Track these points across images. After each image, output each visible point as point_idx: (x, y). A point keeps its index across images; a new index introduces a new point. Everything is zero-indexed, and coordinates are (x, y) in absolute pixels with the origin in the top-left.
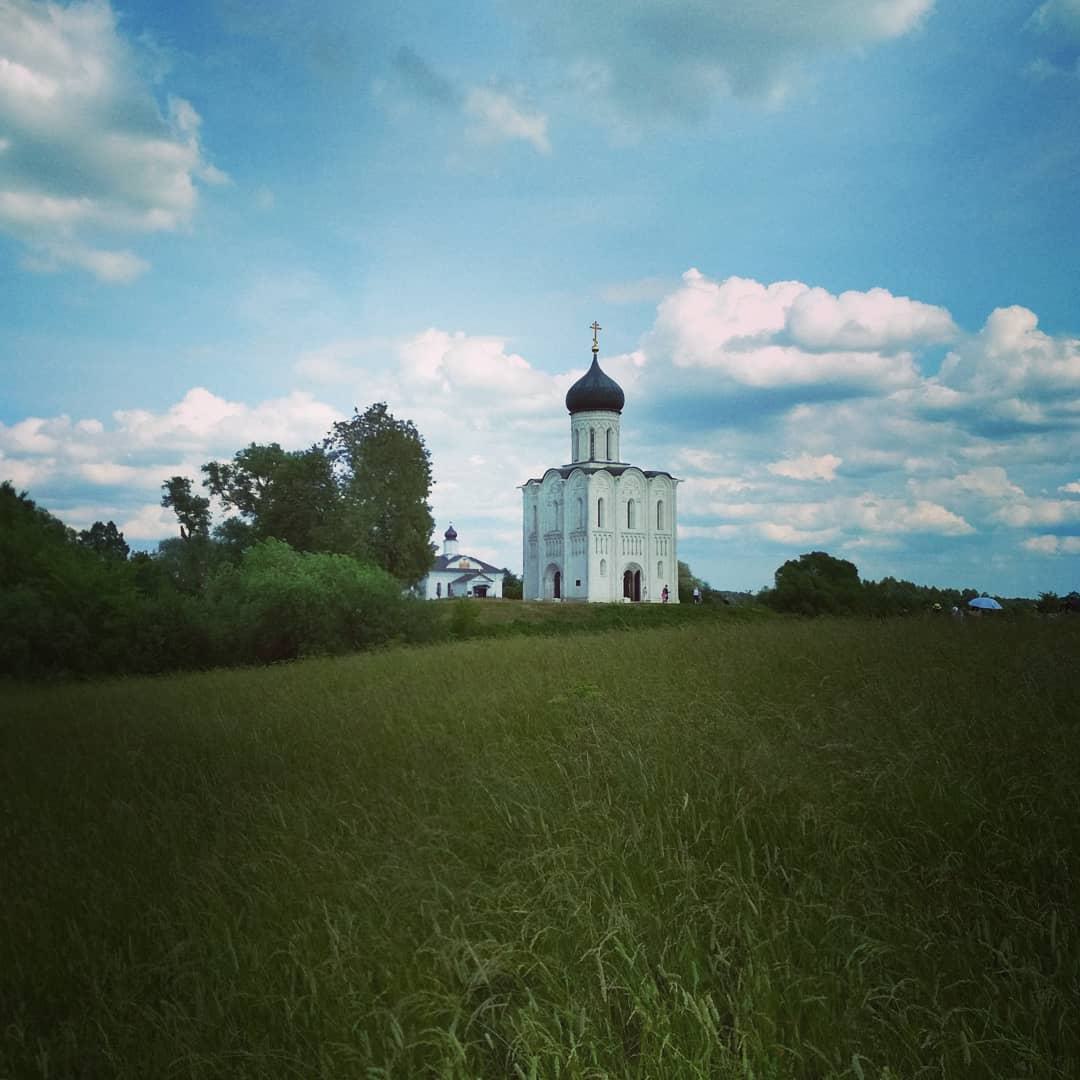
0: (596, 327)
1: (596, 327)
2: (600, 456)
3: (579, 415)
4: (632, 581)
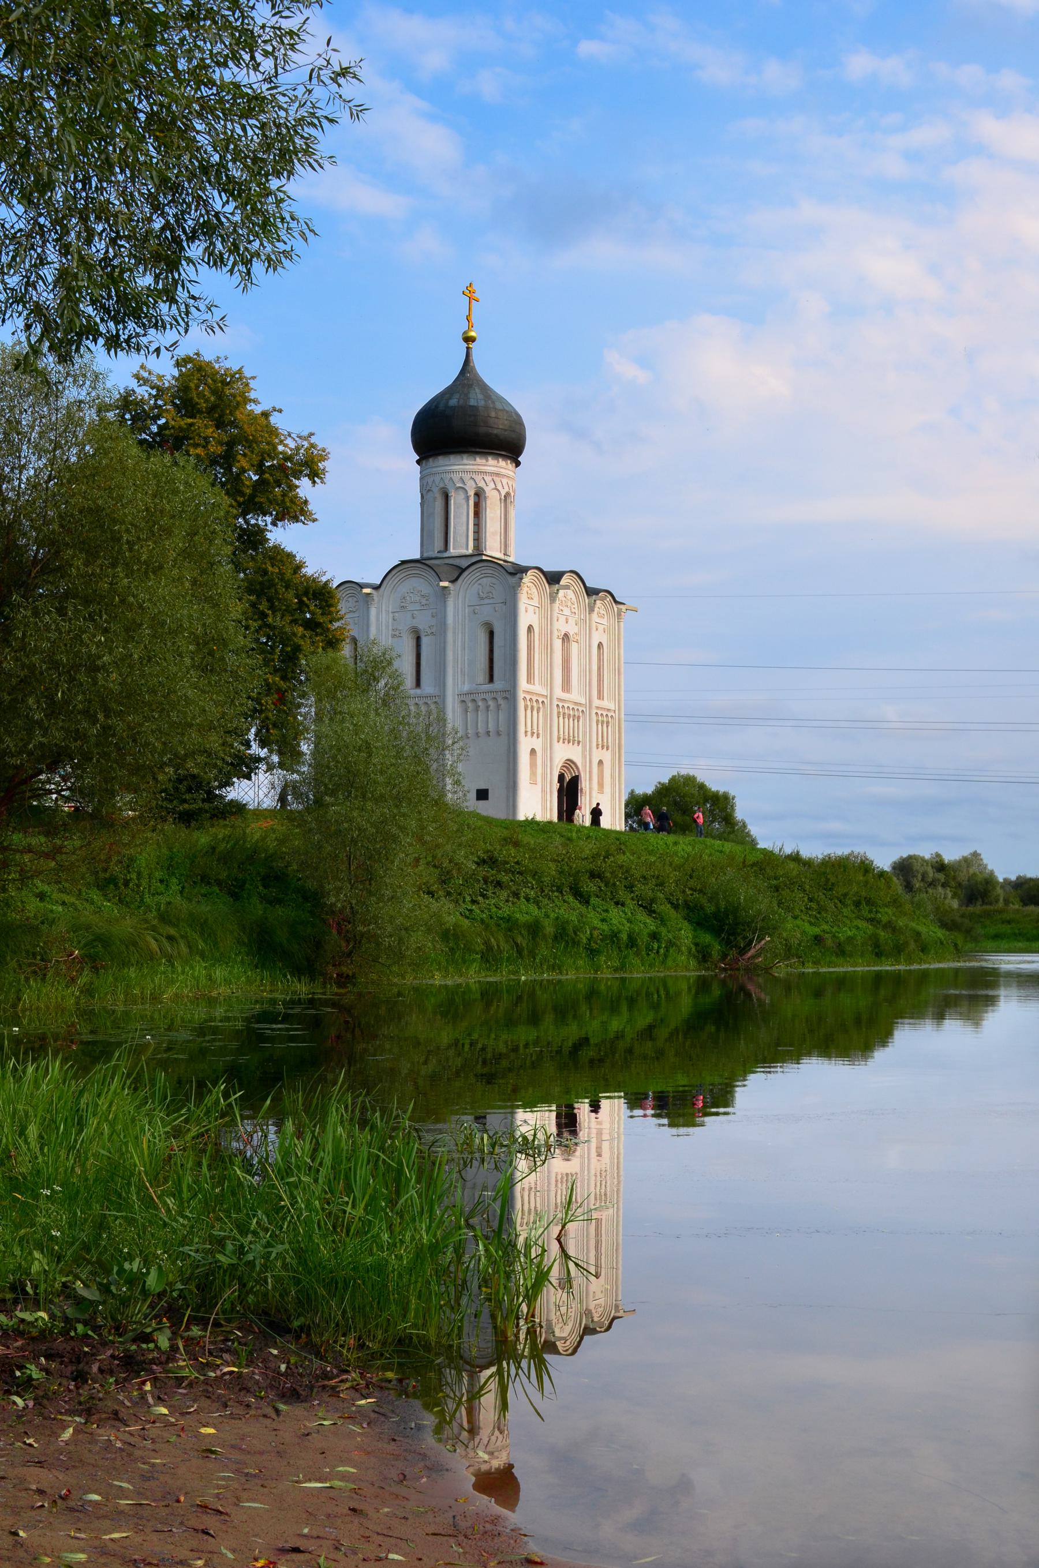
0: (470, 294)
1: (470, 294)
2: (493, 549)
3: (441, 460)
4: (569, 791)
